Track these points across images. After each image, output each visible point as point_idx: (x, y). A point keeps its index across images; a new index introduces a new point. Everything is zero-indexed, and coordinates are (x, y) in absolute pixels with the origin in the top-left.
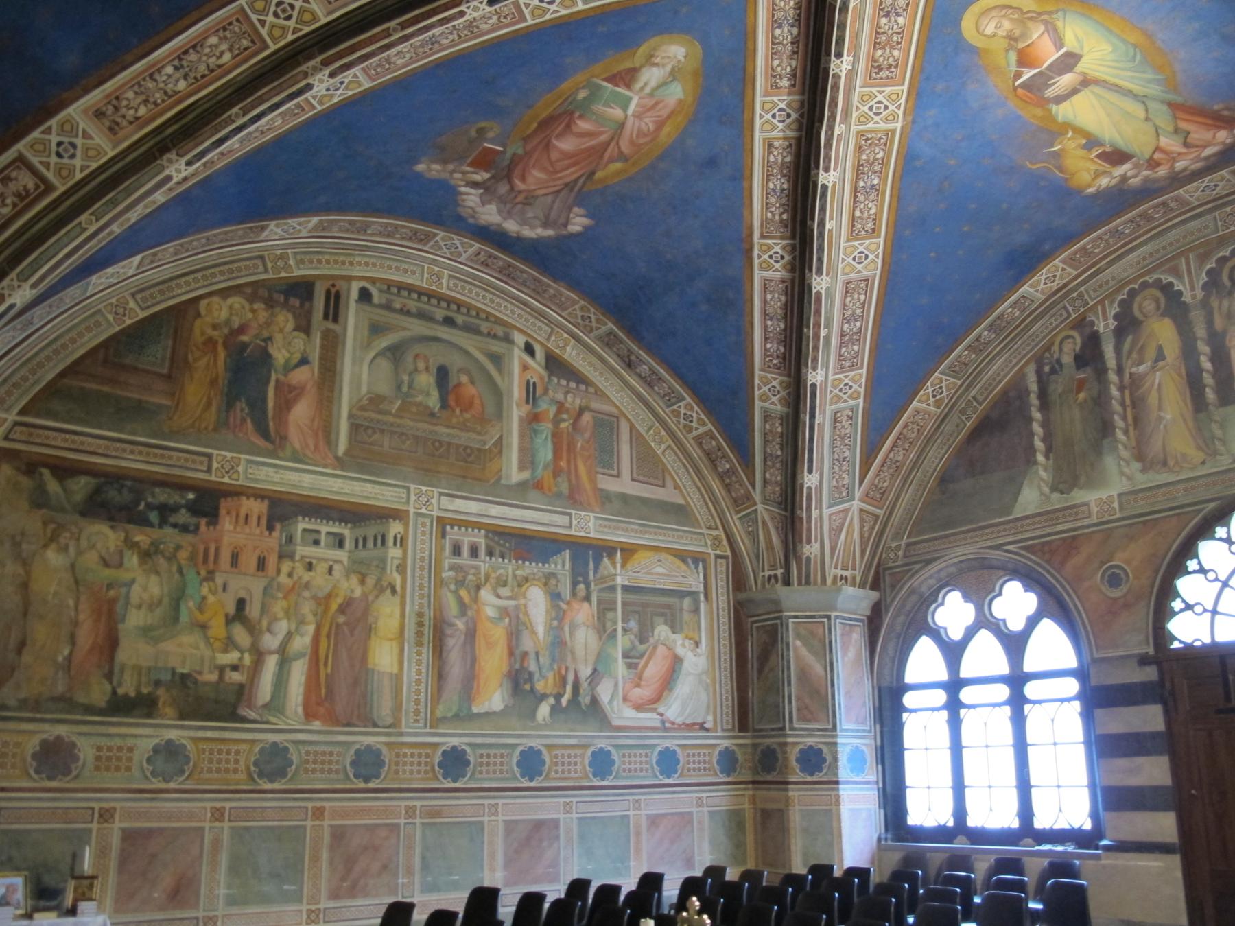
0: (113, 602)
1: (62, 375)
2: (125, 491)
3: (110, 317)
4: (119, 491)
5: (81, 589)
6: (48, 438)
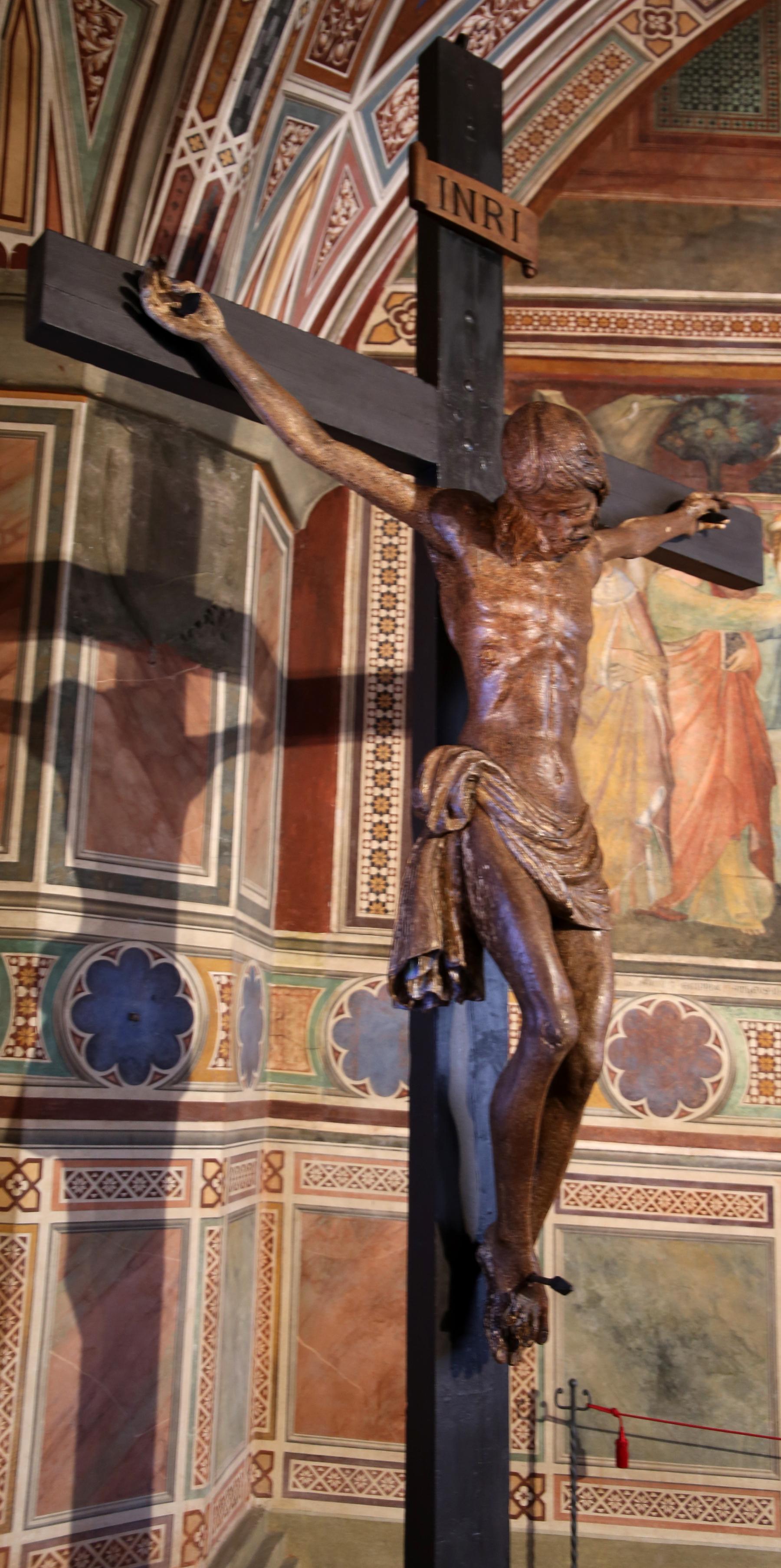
0: (750, 675)
1: (556, 182)
2: (735, 417)
3: (638, 42)
4: (722, 418)
5: (669, 651)
6: (546, 322)
